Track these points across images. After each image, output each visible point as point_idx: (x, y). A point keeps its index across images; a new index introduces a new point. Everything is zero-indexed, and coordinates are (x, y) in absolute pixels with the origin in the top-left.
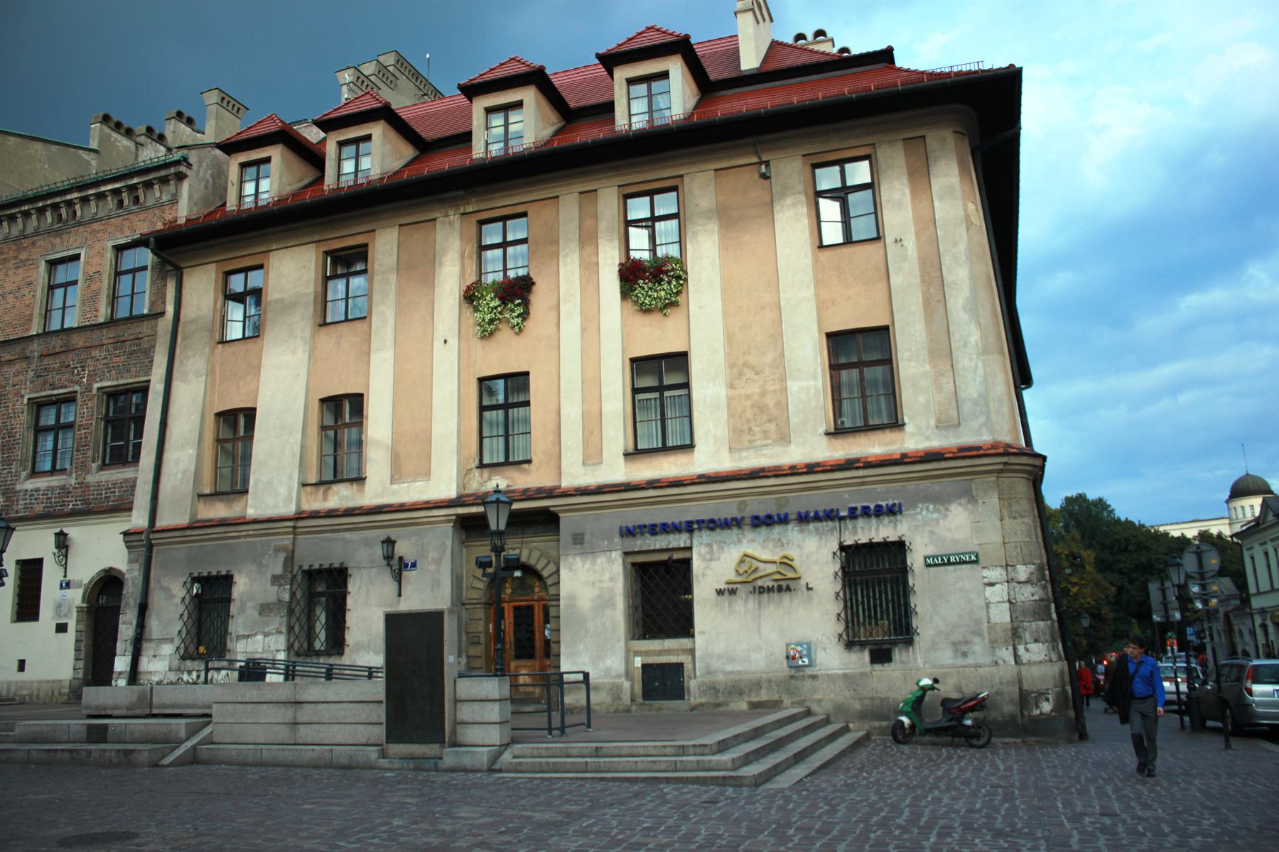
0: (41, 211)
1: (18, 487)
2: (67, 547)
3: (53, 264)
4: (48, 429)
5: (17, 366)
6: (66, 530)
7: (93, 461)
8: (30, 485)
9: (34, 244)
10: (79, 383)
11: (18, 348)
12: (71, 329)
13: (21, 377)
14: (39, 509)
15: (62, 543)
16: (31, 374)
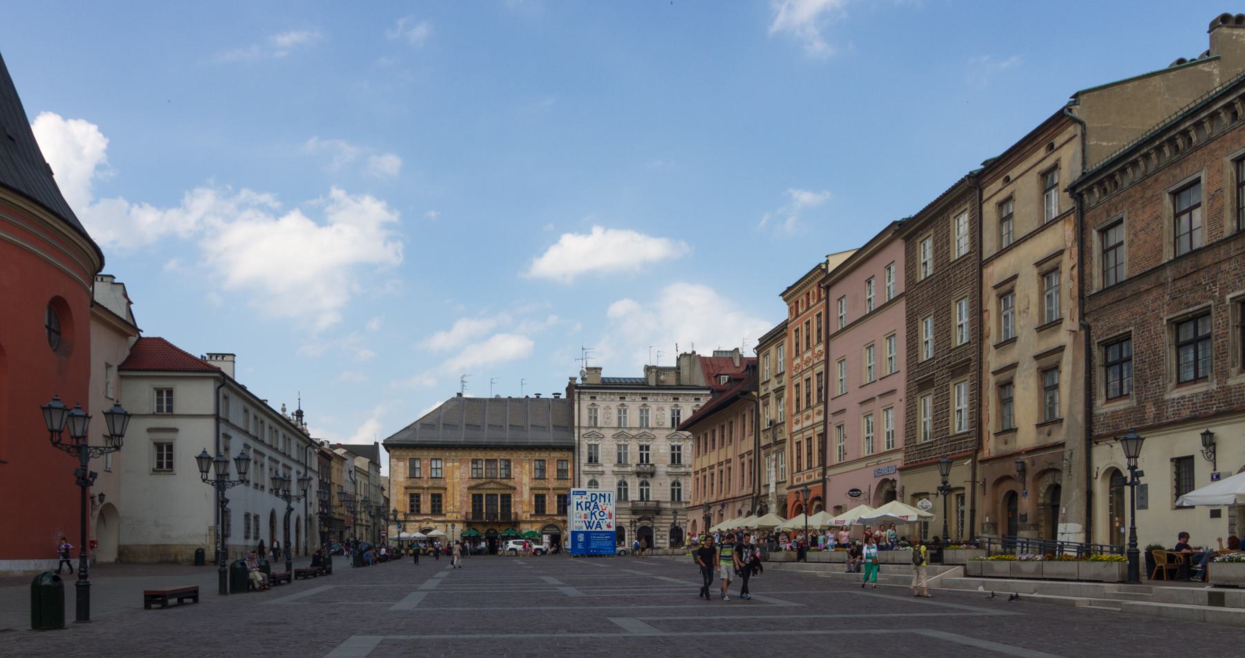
0: (1159, 149)
1: (1167, 397)
2: (1214, 444)
3: (1175, 194)
4: (1187, 344)
5: (1154, 294)
6: (1211, 430)
7: (1233, 366)
8: (1176, 394)
9: (1156, 180)
10: (1212, 297)
11: (1153, 278)
12: (1200, 250)
13: (1159, 302)
14: (1186, 413)
15: (1210, 442)
16: (1167, 298)
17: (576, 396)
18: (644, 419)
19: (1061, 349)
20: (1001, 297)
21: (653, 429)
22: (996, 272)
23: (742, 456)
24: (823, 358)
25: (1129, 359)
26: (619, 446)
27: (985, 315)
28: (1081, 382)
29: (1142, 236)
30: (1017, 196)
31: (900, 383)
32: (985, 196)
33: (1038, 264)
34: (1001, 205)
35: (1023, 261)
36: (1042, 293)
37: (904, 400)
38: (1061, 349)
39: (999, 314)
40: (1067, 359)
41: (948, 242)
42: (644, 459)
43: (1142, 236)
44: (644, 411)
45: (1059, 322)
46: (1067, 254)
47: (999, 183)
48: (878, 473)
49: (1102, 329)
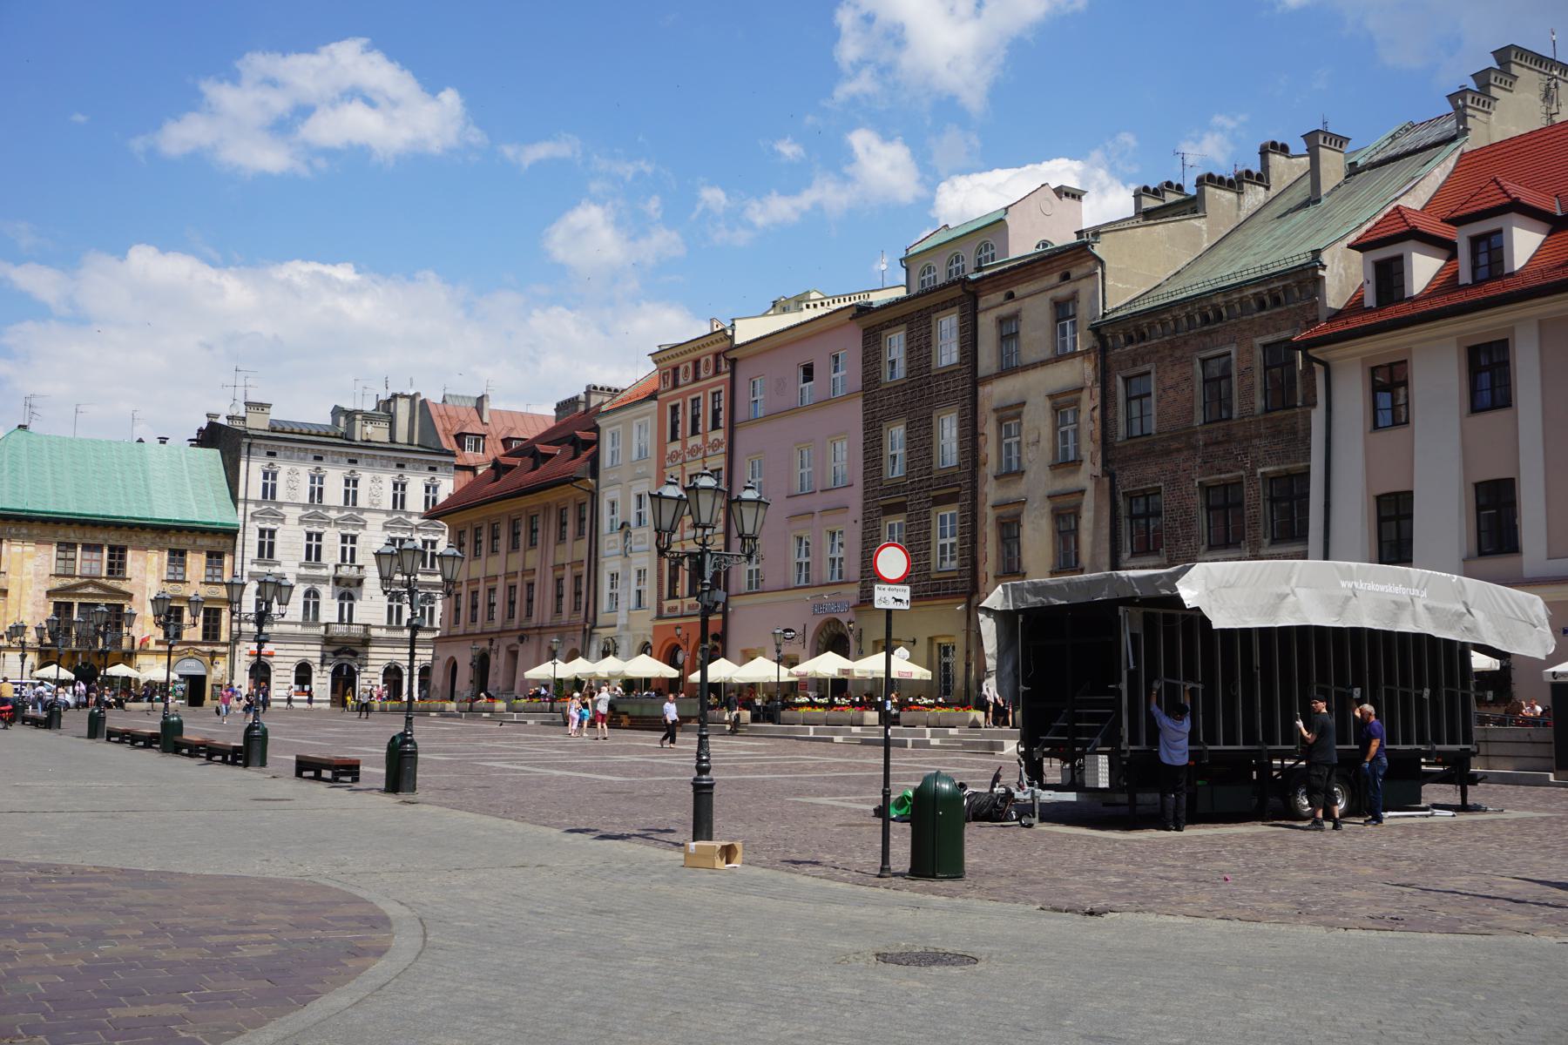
17: (244, 450)
18: (350, 497)
19: (1082, 492)
20: (1000, 422)
21: (363, 510)
22: (994, 394)
23: (556, 568)
24: (723, 449)
25: (1158, 514)
27: (981, 439)
28: (1106, 531)
29: (1171, 393)
30: (1024, 314)
31: (855, 498)
32: (982, 304)
33: (1051, 396)
34: (1001, 321)
35: (1034, 387)
36: (1056, 429)
37: (860, 522)
38: (1082, 492)
39: (1000, 441)
40: (1088, 503)
41: (929, 345)
42: (348, 556)
43: (1171, 393)
44: (351, 482)
45: (1077, 463)
46: (1085, 395)
47: (999, 297)
48: (818, 608)
49: (1126, 481)
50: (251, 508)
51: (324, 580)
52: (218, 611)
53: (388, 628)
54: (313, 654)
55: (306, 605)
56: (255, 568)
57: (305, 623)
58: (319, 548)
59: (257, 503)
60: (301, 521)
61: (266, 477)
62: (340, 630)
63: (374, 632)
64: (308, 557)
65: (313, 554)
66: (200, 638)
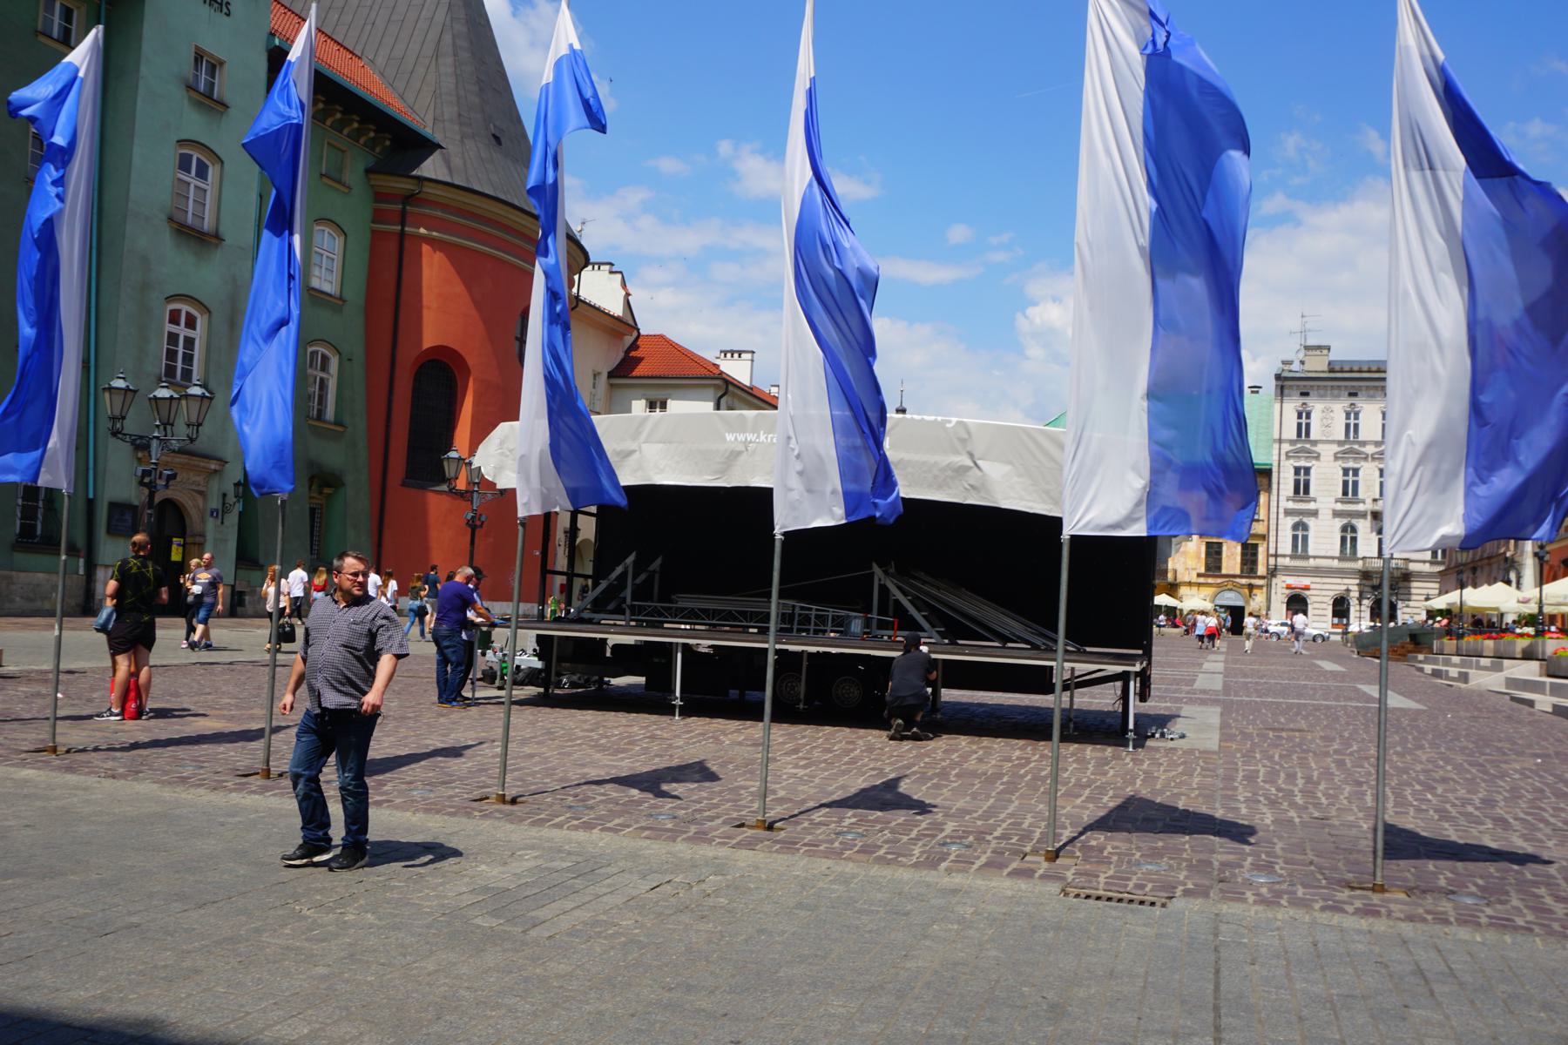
26: (1346, 471)
50: (1286, 447)
51: (1363, 515)
52: (1255, 546)
53: (1431, 563)
54: (1353, 584)
55: (1343, 540)
56: (1291, 505)
57: (1342, 558)
58: (1355, 484)
59: (1292, 442)
60: (1336, 458)
61: (1300, 416)
62: (1378, 564)
63: (1413, 567)
64: (1345, 493)
65: (1349, 490)
66: (1238, 572)
